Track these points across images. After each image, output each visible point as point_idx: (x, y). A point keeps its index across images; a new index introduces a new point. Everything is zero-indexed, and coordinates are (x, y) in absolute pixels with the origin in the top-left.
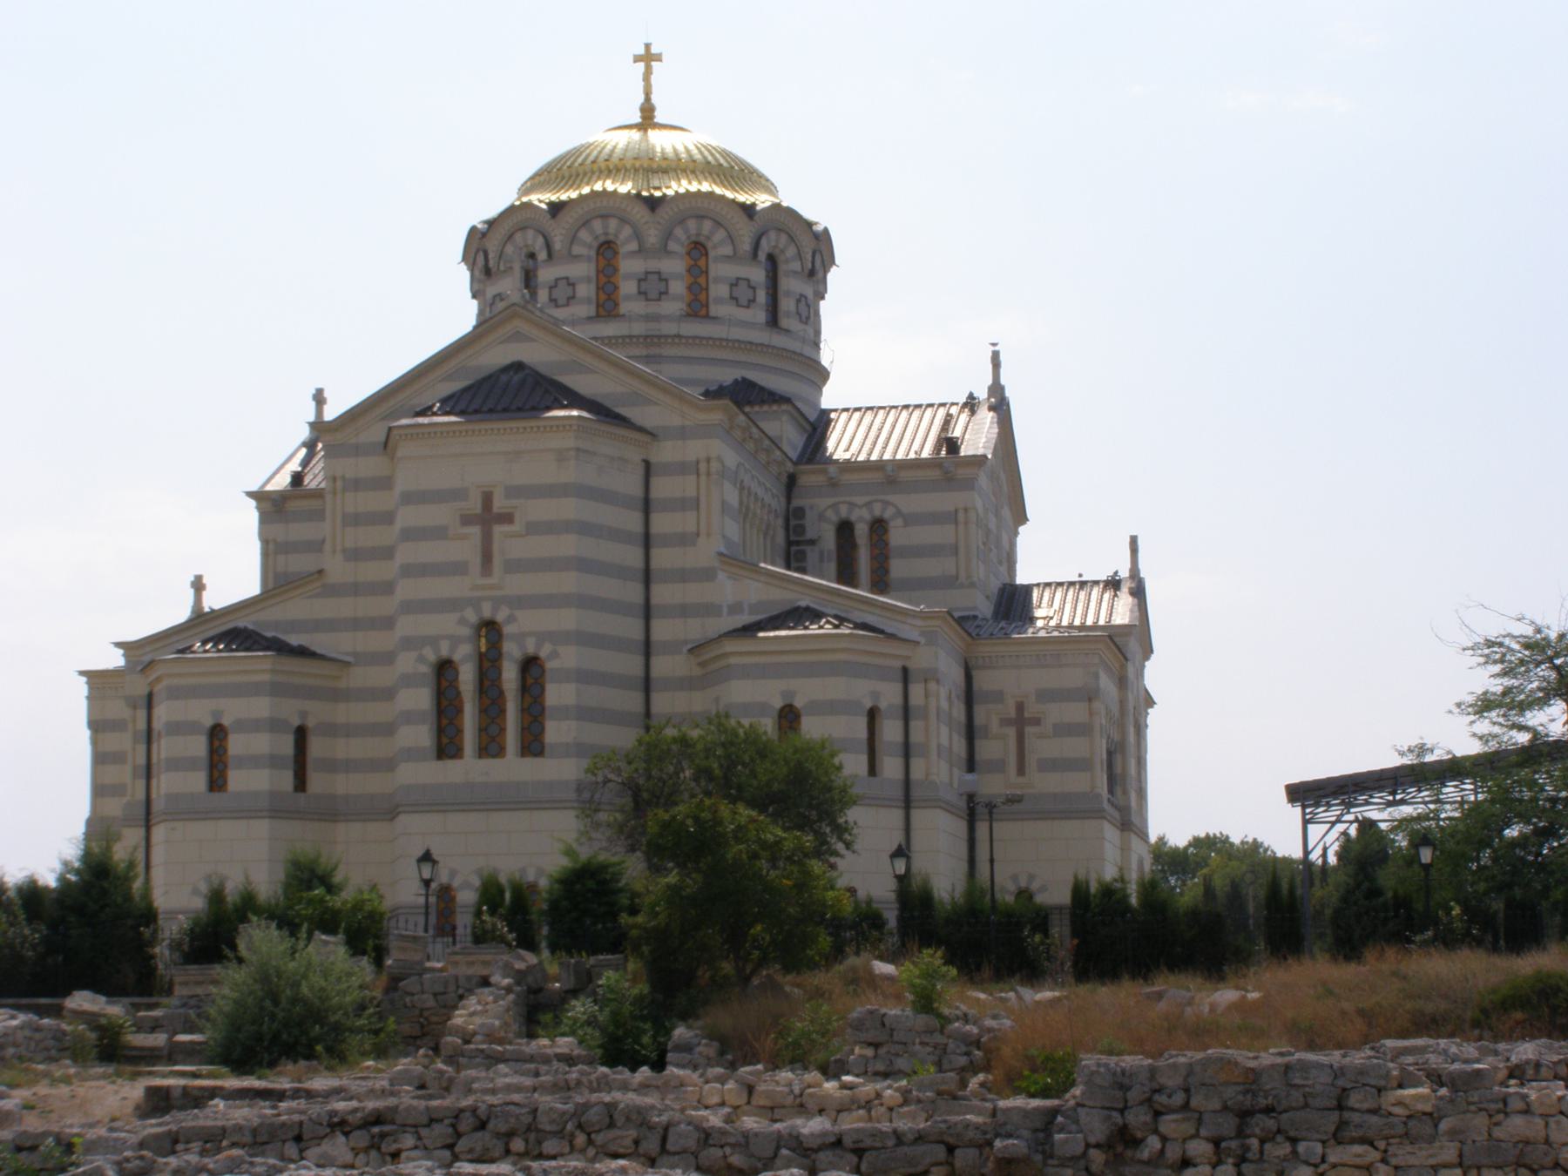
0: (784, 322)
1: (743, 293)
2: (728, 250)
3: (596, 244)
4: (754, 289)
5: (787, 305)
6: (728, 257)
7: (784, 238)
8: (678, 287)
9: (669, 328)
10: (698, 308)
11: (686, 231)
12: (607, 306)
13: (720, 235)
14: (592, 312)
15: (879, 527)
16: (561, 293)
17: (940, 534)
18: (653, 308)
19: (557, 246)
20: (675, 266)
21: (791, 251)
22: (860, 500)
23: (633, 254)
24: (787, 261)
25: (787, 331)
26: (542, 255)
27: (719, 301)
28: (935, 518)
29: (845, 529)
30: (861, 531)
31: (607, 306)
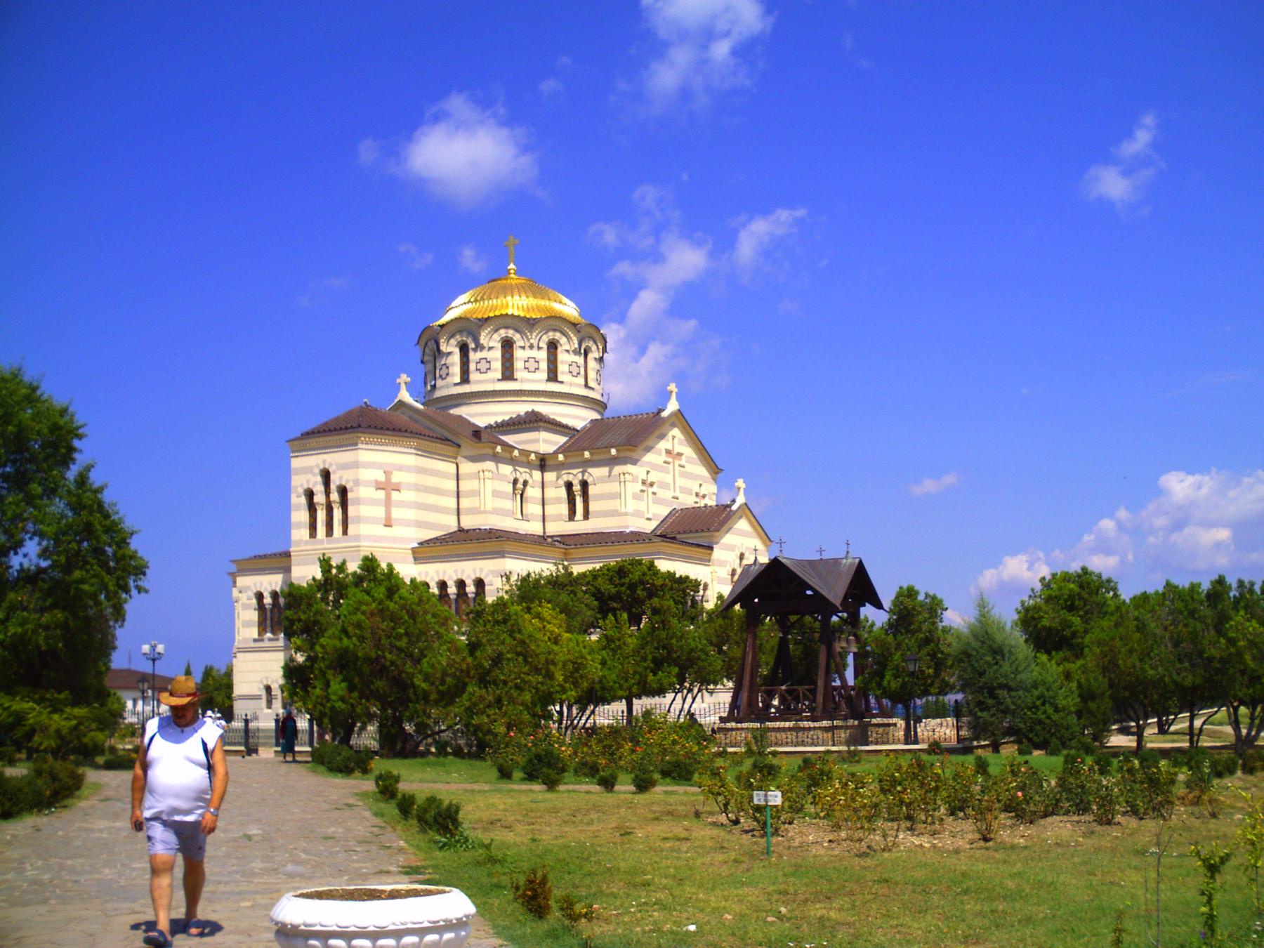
0: (560, 378)
1: (532, 365)
2: (522, 344)
5: (562, 368)
8: (497, 365)
9: (489, 387)
10: (508, 374)
12: (465, 379)
14: (457, 379)
15: (585, 485)
16: (444, 371)
18: (484, 376)
20: (497, 354)
21: (563, 340)
22: (575, 471)
23: (475, 350)
25: (562, 382)
29: (569, 486)
30: (577, 488)
31: (465, 379)
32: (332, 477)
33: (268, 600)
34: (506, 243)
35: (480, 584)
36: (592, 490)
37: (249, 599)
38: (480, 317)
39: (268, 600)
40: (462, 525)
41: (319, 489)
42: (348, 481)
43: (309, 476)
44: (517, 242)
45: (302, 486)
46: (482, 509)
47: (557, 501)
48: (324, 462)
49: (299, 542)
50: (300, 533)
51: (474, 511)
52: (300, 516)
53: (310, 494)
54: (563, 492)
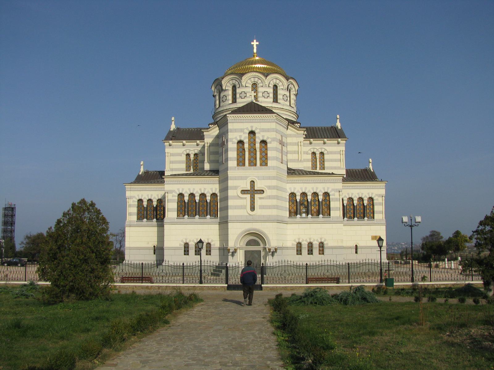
1: (285, 97)
3: (252, 84)
4: (287, 97)
5: (293, 102)
6: (283, 89)
7: (292, 86)
8: (271, 95)
10: (275, 100)
11: (273, 82)
13: (280, 84)
15: (322, 154)
17: (337, 157)
19: (244, 84)
20: (271, 90)
21: (294, 89)
22: (318, 148)
24: (293, 91)
26: (238, 86)
27: (280, 99)
28: (335, 153)
29: (314, 153)
32: (257, 135)
33: (186, 199)
34: (252, 43)
35: (326, 194)
36: (326, 157)
37: (173, 196)
38: (241, 73)
39: (186, 199)
40: (288, 167)
41: (246, 141)
42: (268, 138)
43: (241, 134)
44: (258, 43)
45: (236, 138)
46: (300, 159)
47: (307, 160)
48: (252, 127)
49: (233, 168)
50: (232, 163)
51: (293, 161)
52: (232, 154)
53: (241, 142)
54: (309, 157)
